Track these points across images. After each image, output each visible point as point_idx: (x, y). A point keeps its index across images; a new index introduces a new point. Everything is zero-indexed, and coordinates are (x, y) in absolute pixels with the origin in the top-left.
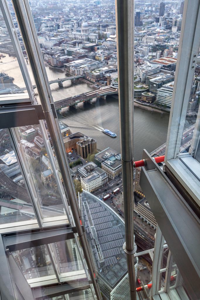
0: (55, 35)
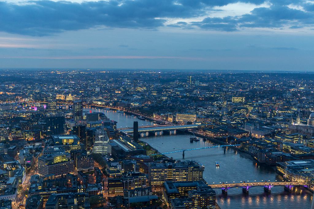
0: (268, 123)
